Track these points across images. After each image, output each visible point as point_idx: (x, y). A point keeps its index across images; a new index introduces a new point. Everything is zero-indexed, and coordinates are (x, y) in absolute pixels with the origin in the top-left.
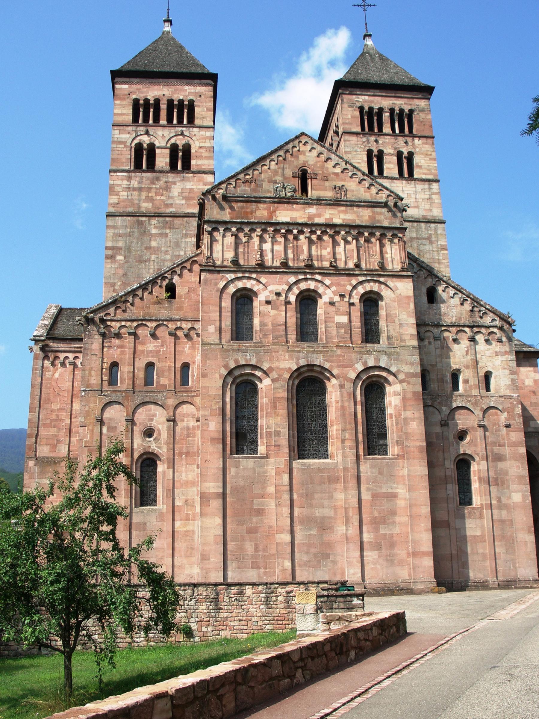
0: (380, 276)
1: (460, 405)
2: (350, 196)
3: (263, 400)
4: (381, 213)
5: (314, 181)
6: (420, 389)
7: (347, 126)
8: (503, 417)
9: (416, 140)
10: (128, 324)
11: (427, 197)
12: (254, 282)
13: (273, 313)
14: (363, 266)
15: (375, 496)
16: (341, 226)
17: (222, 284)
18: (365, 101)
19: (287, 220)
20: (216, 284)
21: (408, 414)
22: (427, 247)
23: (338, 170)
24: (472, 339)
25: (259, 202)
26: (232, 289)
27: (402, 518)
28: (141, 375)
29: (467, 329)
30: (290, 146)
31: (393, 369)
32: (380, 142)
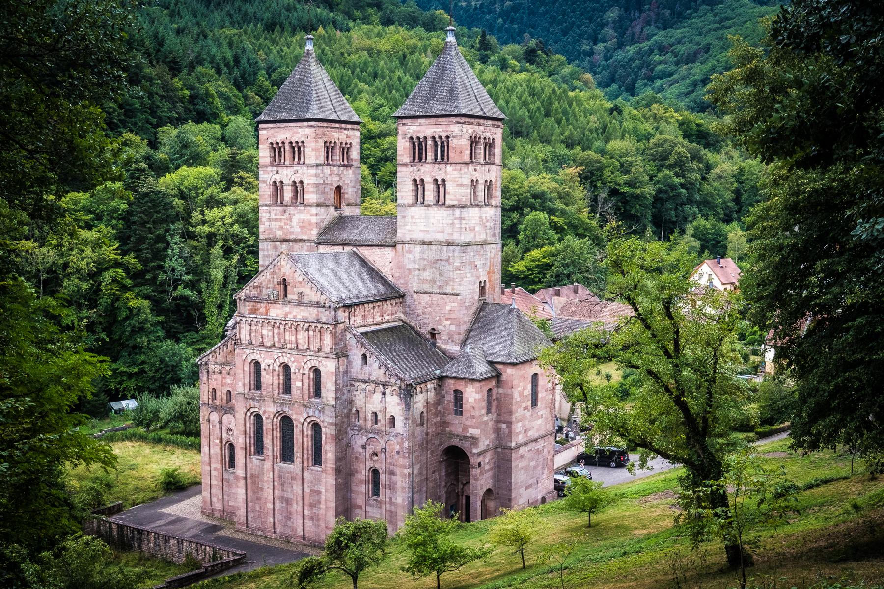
2: (306, 300)
9: (449, 168)
11: (451, 222)
15: (312, 491)
17: (244, 356)
22: (449, 268)
23: (300, 279)
24: (384, 394)
27: (323, 506)
28: (225, 397)
30: (276, 261)
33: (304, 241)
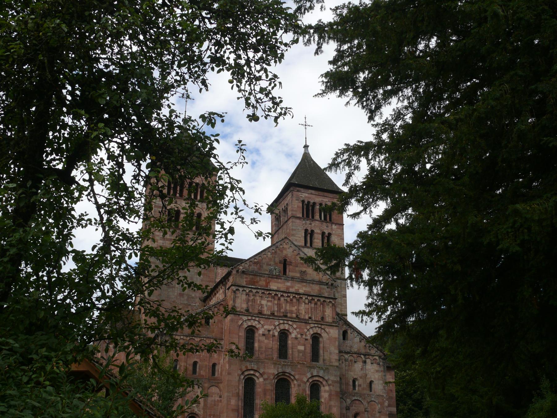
0: (321, 324)
1: (356, 398)
2: (308, 278)
3: (258, 390)
4: (324, 289)
5: (291, 267)
6: (338, 390)
7: (294, 213)
8: (378, 407)
9: (334, 226)
10: (185, 338)
12: (257, 322)
13: (266, 341)
14: (313, 318)
16: (304, 294)
17: (240, 322)
18: (306, 197)
19: (275, 288)
20: (237, 322)
21: (332, 403)
25: (261, 276)
26: (245, 326)
28: (191, 368)
29: (362, 356)
31: (326, 378)
32: (313, 225)
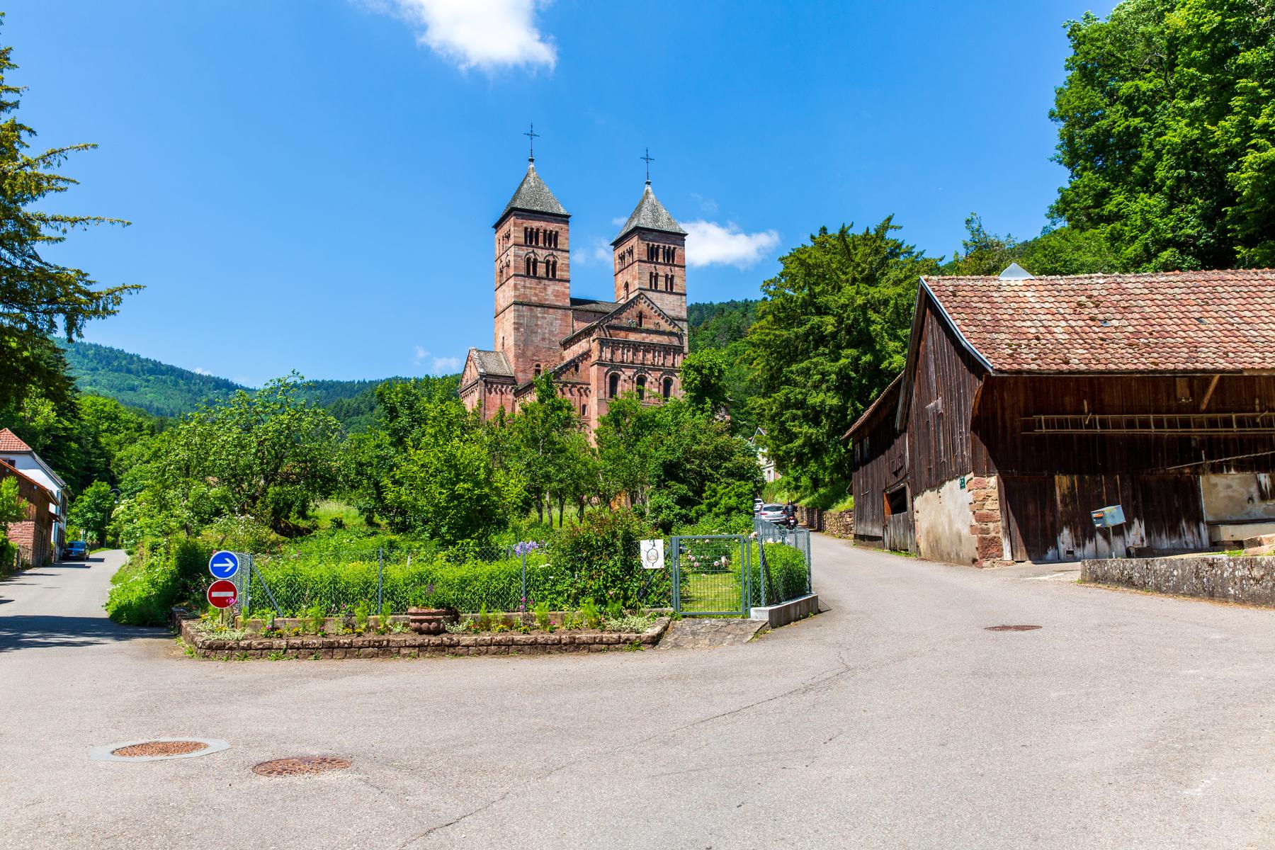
33: (559, 308)
